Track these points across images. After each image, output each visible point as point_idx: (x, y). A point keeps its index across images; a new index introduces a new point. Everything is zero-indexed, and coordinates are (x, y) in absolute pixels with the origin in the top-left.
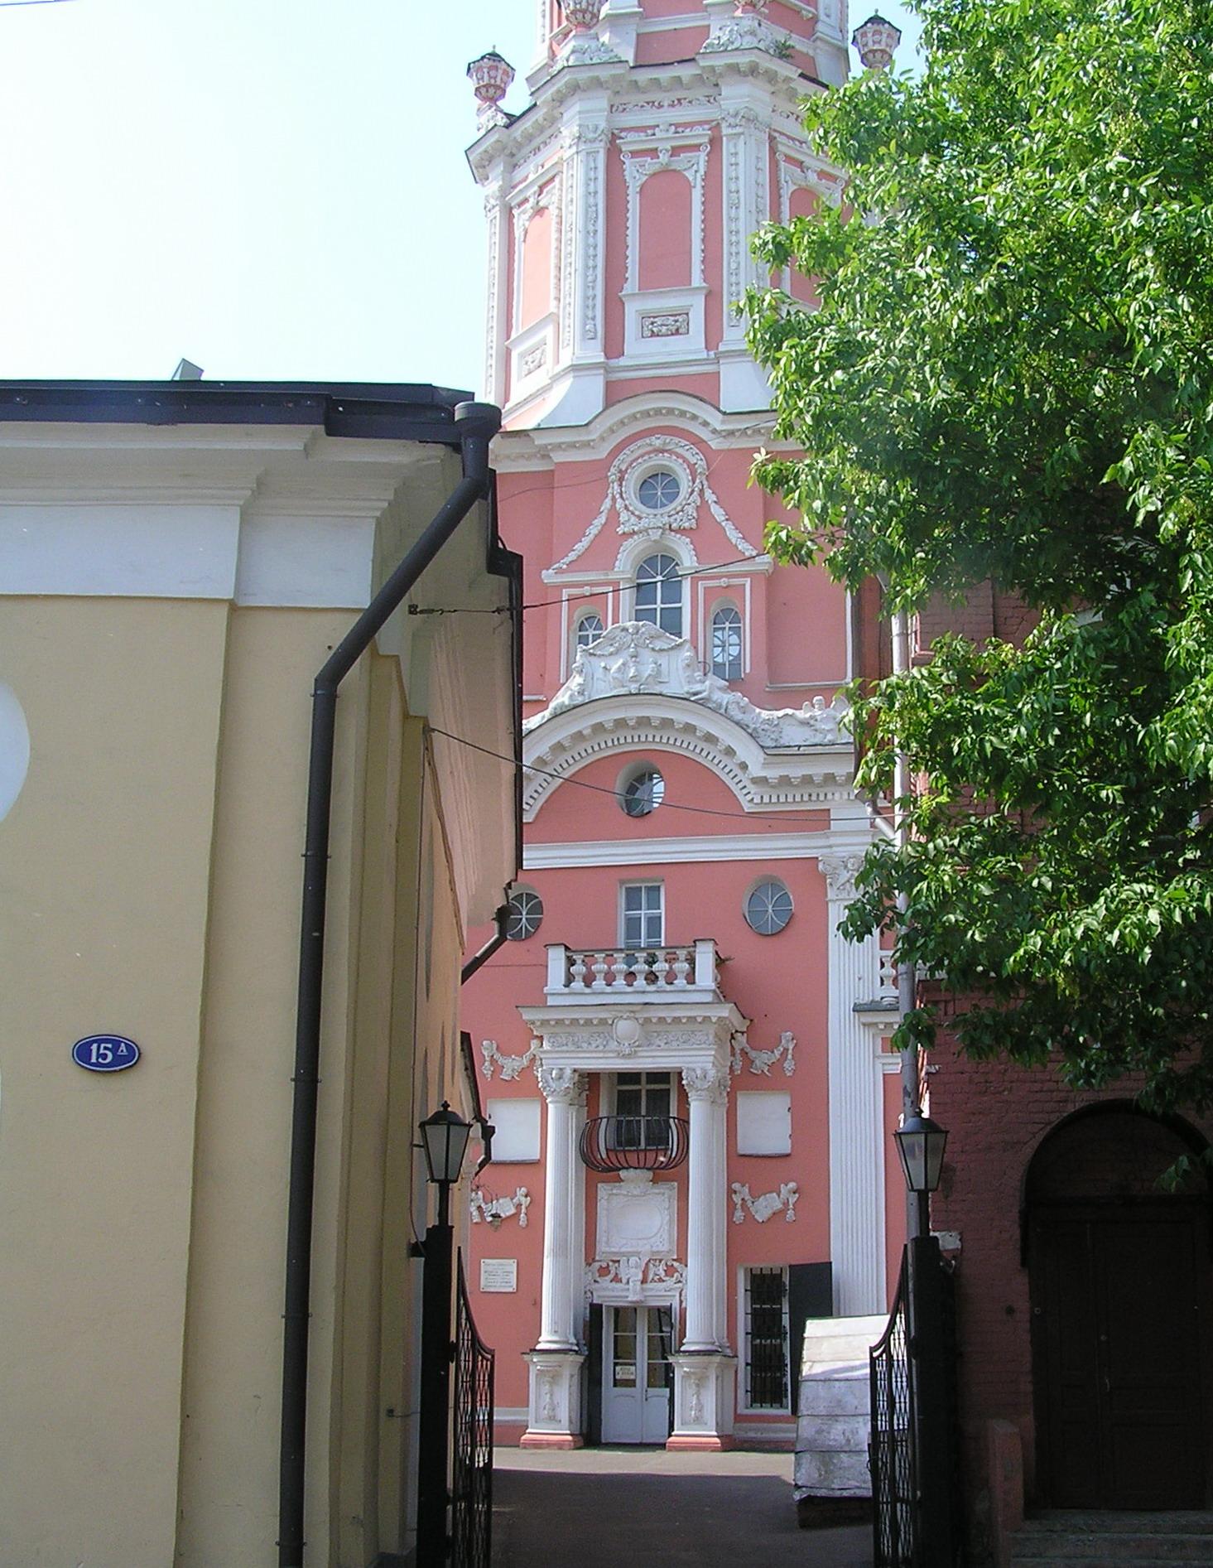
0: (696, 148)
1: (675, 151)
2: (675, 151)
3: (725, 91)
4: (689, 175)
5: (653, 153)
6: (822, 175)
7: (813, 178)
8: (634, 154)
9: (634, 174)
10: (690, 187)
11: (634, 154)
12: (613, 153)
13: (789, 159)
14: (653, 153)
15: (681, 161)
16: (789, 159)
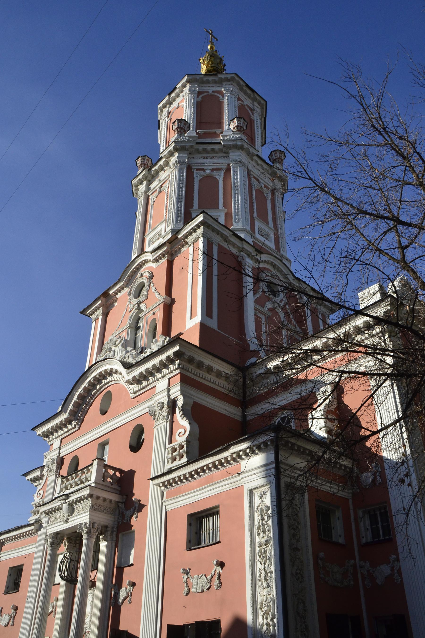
0: (220, 169)
1: (213, 170)
2: (213, 170)
3: (231, 154)
4: (217, 177)
5: (204, 170)
6: (265, 186)
7: (263, 186)
8: (197, 170)
9: (197, 177)
10: (217, 182)
11: (197, 170)
12: (189, 169)
13: (255, 178)
14: (204, 170)
15: (215, 173)
16: (255, 178)
